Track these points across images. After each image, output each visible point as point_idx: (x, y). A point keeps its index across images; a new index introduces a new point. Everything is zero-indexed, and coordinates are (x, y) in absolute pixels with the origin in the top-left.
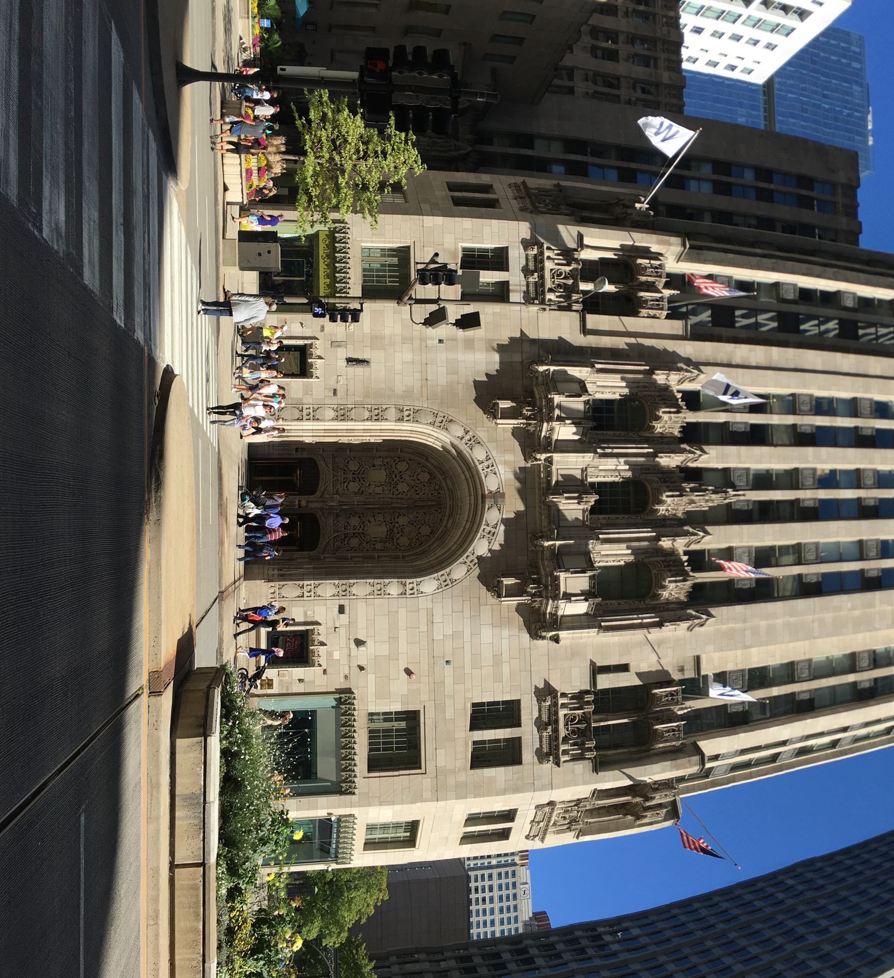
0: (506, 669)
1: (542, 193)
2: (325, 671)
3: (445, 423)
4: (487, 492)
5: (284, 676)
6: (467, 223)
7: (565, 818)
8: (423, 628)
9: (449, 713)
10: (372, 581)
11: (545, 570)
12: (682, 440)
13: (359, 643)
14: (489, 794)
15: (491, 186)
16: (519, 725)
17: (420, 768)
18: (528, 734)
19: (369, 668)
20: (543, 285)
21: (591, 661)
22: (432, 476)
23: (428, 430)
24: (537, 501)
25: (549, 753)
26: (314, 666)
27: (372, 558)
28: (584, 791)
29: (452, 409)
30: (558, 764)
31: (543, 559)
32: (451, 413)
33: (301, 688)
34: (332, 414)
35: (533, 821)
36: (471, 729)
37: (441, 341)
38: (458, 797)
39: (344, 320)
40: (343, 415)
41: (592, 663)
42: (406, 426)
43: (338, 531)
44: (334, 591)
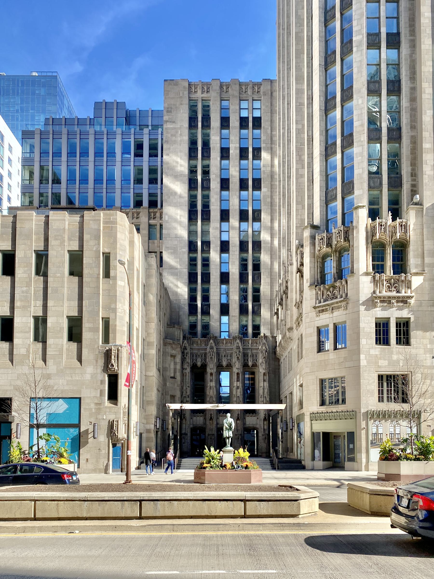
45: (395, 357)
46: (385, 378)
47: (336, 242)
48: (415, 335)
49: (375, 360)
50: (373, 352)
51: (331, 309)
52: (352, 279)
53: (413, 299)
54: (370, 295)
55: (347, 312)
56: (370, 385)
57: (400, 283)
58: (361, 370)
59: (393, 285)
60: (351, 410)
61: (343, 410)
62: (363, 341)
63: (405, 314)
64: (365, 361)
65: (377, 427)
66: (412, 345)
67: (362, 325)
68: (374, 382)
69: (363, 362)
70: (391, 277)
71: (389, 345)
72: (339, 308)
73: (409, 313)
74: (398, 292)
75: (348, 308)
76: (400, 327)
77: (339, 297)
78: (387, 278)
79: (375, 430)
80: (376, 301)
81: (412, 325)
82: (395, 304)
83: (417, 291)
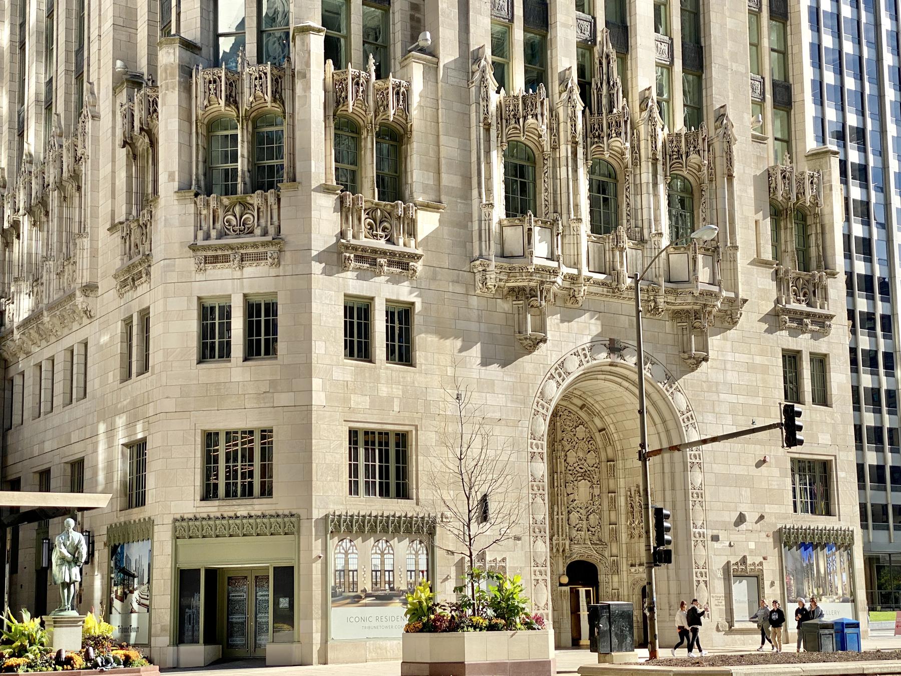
0: (758, 360)
2: (765, 559)
4: (609, 360)
11: (689, 304)
13: (741, 519)
17: (831, 461)
19: (761, 512)
21: (750, 264)
24: (616, 301)
26: (762, 570)
29: (531, 391)
33: (777, 583)
45: (384, 390)
46: (361, 439)
47: (251, 99)
48: (425, 343)
49: (341, 394)
51: (238, 258)
52: (292, 194)
53: (420, 262)
54: (334, 240)
55: (281, 271)
56: (331, 454)
57: (394, 222)
59: (381, 223)
60: (287, 512)
61: (267, 513)
62: (319, 348)
63: (404, 292)
66: (418, 366)
67: (316, 307)
68: (341, 444)
69: (318, 398)
70: (376, 204)
71: (370, 362)
72: (259, 258)
73: (411, 293)
74: (389, 241)
75: (282, 263)
77: (258, 231)
78: (369, 205)
80: (348, 255)
81: (417, 320)
82: (386, 268)
83: (427, 245)
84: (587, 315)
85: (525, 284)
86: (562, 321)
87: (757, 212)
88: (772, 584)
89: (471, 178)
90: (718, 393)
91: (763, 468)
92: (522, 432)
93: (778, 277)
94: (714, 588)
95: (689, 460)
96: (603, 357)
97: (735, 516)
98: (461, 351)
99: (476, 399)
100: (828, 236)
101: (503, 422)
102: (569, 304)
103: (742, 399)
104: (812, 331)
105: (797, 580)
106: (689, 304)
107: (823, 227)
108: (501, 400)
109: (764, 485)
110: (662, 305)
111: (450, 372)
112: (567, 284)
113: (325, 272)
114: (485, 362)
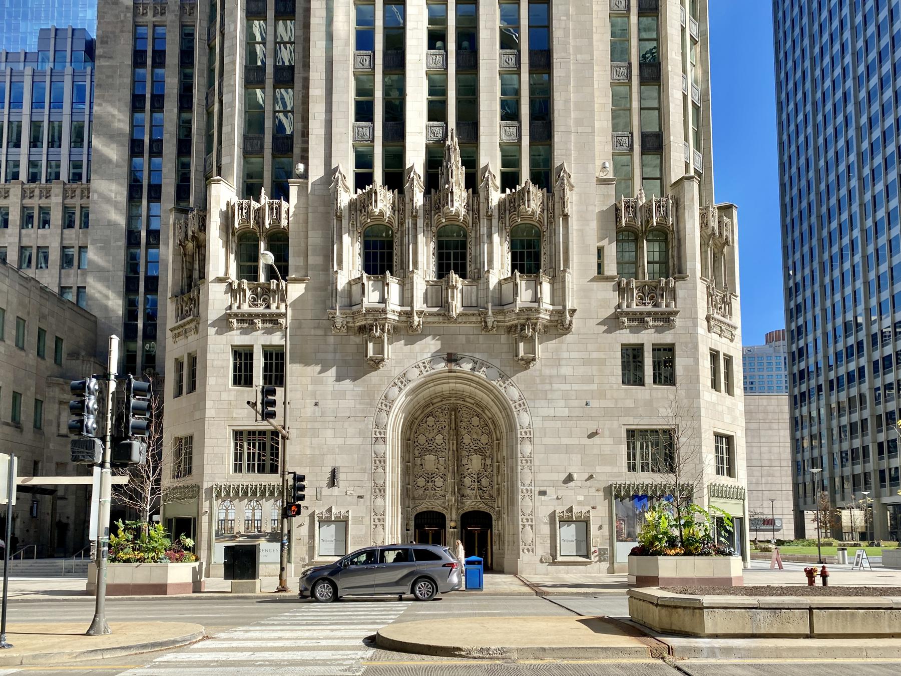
0: (594, 355)
1: (181, 314)
2: (593, 508)
3: (388, 402)
5: (597, 542)
6: (211, 381)
7: (720, 308)
8: (559, 424)
9: (630, 403)
10: (519, 468)
11: (514, 320)
12: (401, 192)
13: (570, 478)
14: (697, 371)
15: (176, 359)
16: (642, 345)
18: (648, 338)
20: (264, 315)
22: (431, 414)
23: (392, 416)
25: (666, 319)
27: (498, 467)
28: (701, 288)
30: (676, 313)
31: (504, 322)
32: (379, 397)
33: (606, 528)
34: (379, 501)
35: (720, 335)
36: (643, 385)
37: (316, 404)
38: (698, 397)
39: (302, 488)
40: (380, 491)
41: (593, 280)
42: (389, 436)
43: (476, 496)
44: (527, 498)
50: (225, 396)
58: (206, 423)
63: (276, 339)
64: (213, 411)
65: (227, 509)
76: (271, 359)
79: (224, 514)
84: (430, 338)
85: (364, 323)
86: (406, 345)
87: (601, 239)
88: (600, 528)
89: (329, 257)
90: (551, 384)
91: (596, 439)
92: (367, 424)
93: (621, 290)
94: (539, 531)
95: (519, 436)
96: (442, 366)
97: (564, 476)
98: (320, 373)
99: (328, 404)
100: (682, 247)
101: (352, 419)
102: (410, 332)
103: (575, 387)
104: (654, 327)
105: (628, 525)
106: (514, 320)
107: (679, 240)
108: (351, 404)
109: (596, 451)
110: (490, 324)
111: (310, 388)
112: (404, 318)
113: (217, 333)
114: (339, 378)
